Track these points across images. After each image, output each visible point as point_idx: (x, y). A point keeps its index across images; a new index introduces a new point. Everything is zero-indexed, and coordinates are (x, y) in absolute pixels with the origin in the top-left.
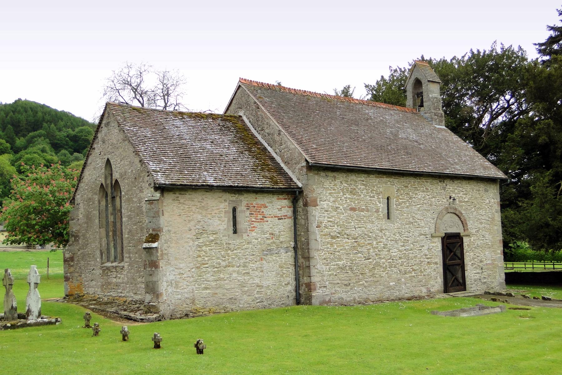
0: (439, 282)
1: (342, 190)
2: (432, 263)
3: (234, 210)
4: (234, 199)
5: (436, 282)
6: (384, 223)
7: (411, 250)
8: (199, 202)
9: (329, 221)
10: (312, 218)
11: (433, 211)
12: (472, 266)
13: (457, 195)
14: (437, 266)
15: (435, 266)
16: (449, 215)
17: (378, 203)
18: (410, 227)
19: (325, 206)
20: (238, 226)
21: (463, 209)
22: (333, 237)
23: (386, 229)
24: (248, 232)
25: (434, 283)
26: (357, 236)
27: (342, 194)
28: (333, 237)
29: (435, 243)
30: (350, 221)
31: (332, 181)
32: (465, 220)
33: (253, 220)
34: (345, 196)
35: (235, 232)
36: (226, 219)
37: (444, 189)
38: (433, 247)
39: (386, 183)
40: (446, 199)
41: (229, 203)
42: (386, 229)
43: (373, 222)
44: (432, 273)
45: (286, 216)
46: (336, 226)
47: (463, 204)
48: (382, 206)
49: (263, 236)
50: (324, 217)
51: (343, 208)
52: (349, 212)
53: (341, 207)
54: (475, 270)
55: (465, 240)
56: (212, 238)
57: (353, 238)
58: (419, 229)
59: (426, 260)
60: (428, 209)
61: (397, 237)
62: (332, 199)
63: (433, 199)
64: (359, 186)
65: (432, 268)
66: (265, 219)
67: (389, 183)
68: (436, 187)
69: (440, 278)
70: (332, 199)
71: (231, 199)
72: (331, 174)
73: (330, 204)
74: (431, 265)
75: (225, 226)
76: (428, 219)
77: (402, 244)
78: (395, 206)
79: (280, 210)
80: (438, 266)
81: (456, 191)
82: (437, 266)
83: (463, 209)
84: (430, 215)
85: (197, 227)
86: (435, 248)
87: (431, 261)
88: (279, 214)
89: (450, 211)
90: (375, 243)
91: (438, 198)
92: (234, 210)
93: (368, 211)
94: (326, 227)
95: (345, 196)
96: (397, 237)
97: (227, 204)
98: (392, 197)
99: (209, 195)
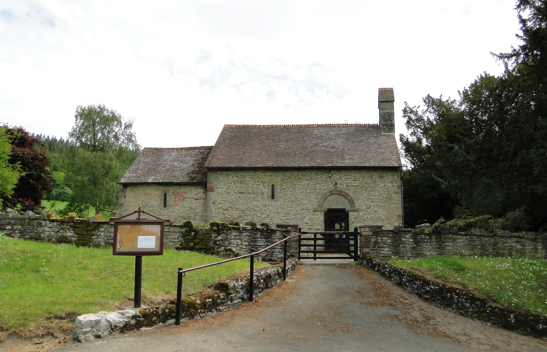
1: (234, 182)
3: (165, 195)
4: (165, 189)
6: (269, 202)
7: (292, 219)
8: (144, 191)
9: (222, 200)
10: (209, 199)
13: (344, 182)
16: (333, 196)
17: (263, 189)
18: (292, 204)
19: (220, 191)
20: (167, 204)
22: (224, 210)
23: (269, 205)
24: (173, 206)
26: (244, 209)
27: (233, 184)
28: (224, 210)
30: (239, 200)
31: (226, 176)
32: (352, 199)
33: (177, 200)
34: (236, 185)
35: (165, 206)
36: (159, 200)
37: (330, 177)
39: (271, 176)
41: (162, 192)
42: (269, 205)
43: (258, 201)
45: (201, 198)
46: (227, 203)
48: (267, 191)
49: (183, 209)
50: (219, 198)
51: (234, 192)
52: (238, 195)
53: (232, 192)
55: (350, 214)
56: (150, 209)
57: (240, 211)
58: (302, 206)
59: (307, 227)
60: (313, 192)
61: (280, 210)
62: (226, 187)
63: (318, 185)
64: (247, 179)
66: (185, 200)
67: (274, 176)
68: (323, 177)
70: (226, 187)
71: (163, 189)
72: (225, 173)
73: (225, 190)
75: (159, 203)
77: (284, 215)
78: (279, 190)
79: (197, 194)
81: (343, 179)
85: (142, 203)
88: (196, 197)
89: (335, 192)
90: (259, 214)
92: (165, 195)
93: (254, 193)
94: (219, 203)
95: (236, 185)
96: (280, 210)
97: (160, 192)
98: (275, 185)
99: (149, 187)
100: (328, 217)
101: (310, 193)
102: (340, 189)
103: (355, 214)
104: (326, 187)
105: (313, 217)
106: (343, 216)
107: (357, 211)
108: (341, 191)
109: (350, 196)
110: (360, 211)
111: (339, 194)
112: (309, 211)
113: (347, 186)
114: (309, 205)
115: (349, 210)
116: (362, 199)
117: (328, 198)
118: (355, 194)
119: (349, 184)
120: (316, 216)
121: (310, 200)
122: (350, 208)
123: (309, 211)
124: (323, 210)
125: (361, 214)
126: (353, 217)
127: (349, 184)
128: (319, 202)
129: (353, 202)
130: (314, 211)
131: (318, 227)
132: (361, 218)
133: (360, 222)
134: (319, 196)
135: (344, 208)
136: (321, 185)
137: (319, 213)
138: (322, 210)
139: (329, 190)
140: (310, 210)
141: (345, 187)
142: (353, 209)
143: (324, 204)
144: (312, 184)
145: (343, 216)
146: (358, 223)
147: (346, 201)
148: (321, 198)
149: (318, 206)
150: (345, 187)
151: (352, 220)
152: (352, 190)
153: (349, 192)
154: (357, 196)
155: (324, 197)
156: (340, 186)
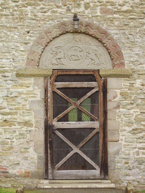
0: (32, 158)
2: (16, 123)
5: (26, 158)
11: (28, 30)
12: (134, 134)
14: (30, 129)
15: (23, 129)
21: (116, 26)
25: (20, 159)
29: (28, 87)
32: (115, 46)
38: (20, 93)
40: (66, 7)
44: (14, 140)
47: (115, 16)
54: (141, 143)
55: (112, 83)
60: (15, 25)
63: (29, 7)
65: (15, 132)
69: (35, 150)
74: (13, 127)
76: (10, 44)
80: (33, 129)
82: (30, 129)
83: (116, 26)
84: (16, 37)
86: (24, 96)
87: (11, 119)
91: (42, 6)
100: (54, 92)
101: (10, 29)
102: (87, 20)
103: (124, 83)
104: (49, 13)
105: (15, 91)
106: (93, 88)
107: (127, 76)
108: (88, 25)
109: (112, 39)
110: (135, 76)
111: (84, 33)
112: (5, 76)
113: (105, 11)
114: (4, 60)
115: (109, 73)
116: (141, 47)
117: (53, 42)
118: (124, 33)
119: (110, 7)
120: (24, 90)
121: (8, 47)
122: (111, 67)
123: (5, 76)
124: (41, 73)
125: (138, 83)
126: (118, 91)
127: (110, 7)
128: (32, 52)
129: (120, 54)
130: (18, 75)
131: (27, 118)
132: (138, 94)
133: (134, 105)
134: (32, 39)
135: (95, 68)
136: (38, 8)
137: (32, 80)
138: (36, 72)
139: (56, 22)
140: (7, 74)
141: (99, 14)
142: (117, 71)
143: (43, 59)
144: (14, 4)
145: (93, 88)
146: (129, 107)
147: (102, 51)
148: (37, 43)
149: (30, 61)
150: (99, 14)
151: (116, 99)
152: (116, 23)
153: (109, 26)
154: (128, 38)
155: (44, 42)
156: (87, 12)
